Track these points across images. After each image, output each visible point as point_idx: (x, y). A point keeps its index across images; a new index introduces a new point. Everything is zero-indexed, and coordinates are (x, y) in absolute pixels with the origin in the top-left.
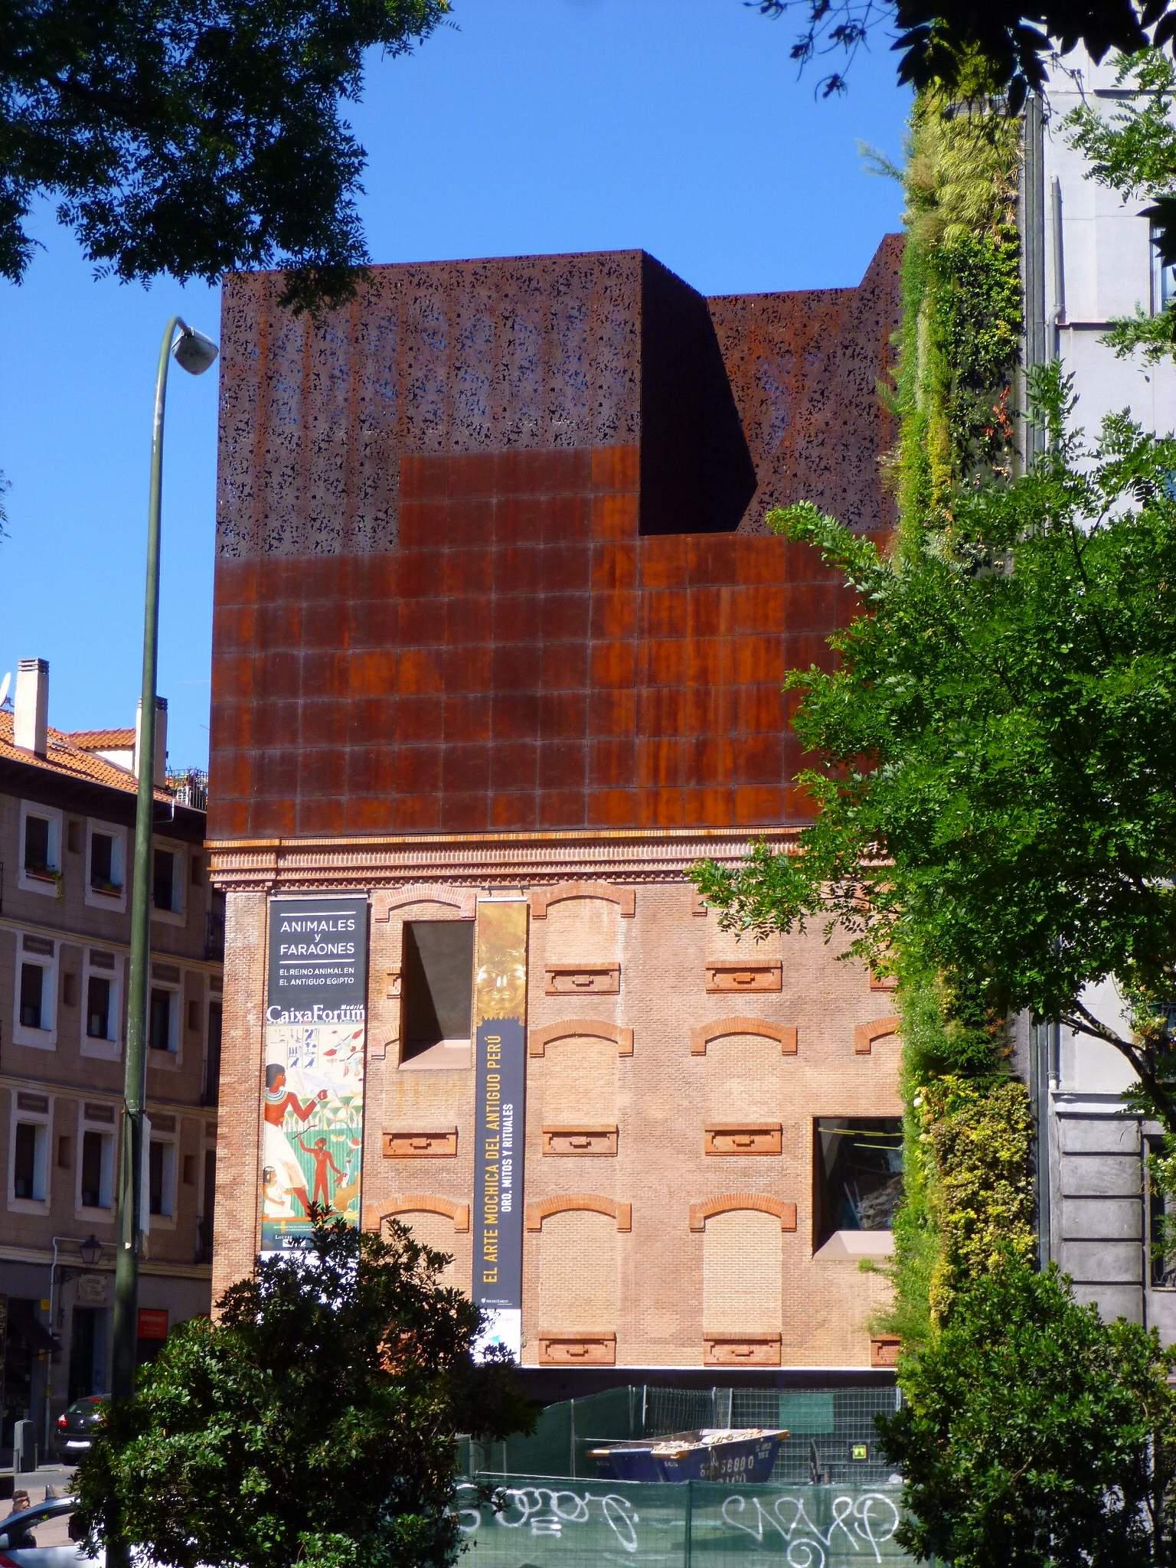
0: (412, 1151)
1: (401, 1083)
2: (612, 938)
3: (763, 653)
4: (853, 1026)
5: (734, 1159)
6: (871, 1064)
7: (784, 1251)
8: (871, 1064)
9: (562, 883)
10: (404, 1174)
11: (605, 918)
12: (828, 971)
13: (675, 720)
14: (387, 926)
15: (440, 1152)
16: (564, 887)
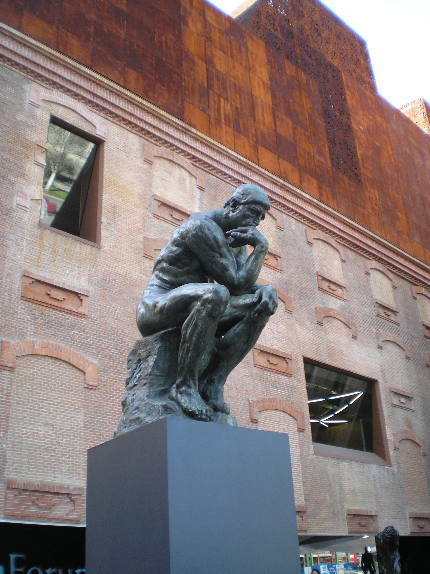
0: (49, 301)
1: (41, 237)
2: (193, 198)
3: (262, 87)
4: (313, 307)
5: (269, 373)
6: (323, 333)
7: (300, 444)
8: (323, 333)
9: (163, 147)
10: (40, 321)
11: (188, 184)
12: (300, 270)
13: (227, 93)
14: (38, 112)
15: (74, 309)
16: (163, 150)
